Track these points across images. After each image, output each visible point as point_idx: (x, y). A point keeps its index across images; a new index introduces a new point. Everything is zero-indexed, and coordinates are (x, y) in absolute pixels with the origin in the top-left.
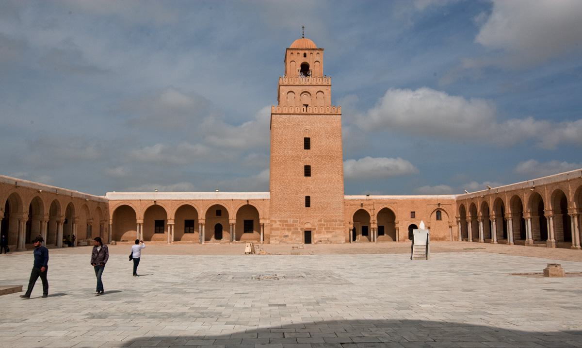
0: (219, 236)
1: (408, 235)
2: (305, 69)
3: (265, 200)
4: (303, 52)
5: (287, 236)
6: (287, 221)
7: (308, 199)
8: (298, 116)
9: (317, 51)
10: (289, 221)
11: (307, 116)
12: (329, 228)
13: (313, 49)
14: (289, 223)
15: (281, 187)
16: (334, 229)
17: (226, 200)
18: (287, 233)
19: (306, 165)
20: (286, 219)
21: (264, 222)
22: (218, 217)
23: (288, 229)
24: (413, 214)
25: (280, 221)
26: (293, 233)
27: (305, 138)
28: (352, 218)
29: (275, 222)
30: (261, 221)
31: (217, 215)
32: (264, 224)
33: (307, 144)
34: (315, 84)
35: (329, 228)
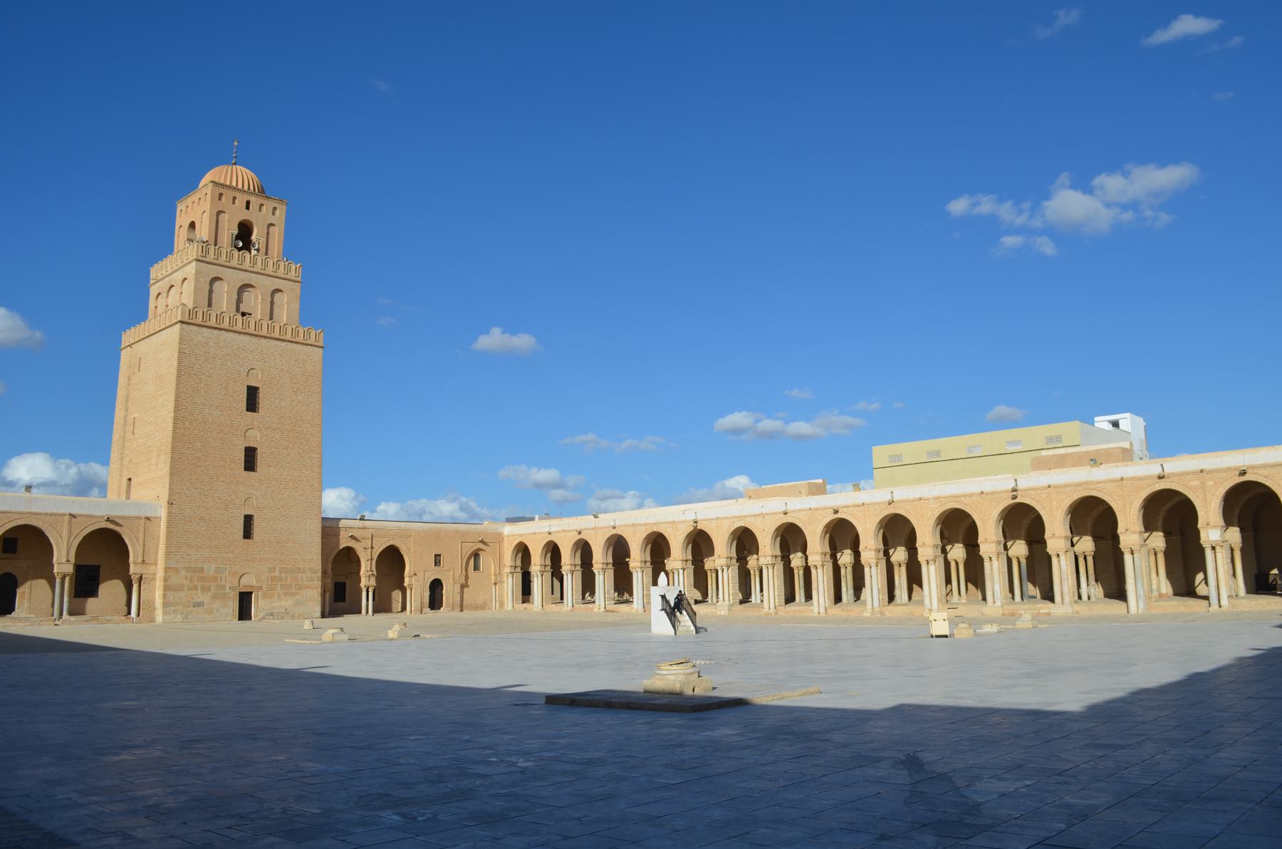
1: (427, 600)
4: (247, 198)
5: (200, 604)
6: (202, 570)
7: (248, 520)
8: (236, 336)
9: (274, 204)
11: (255, 340)
16: (300, 588)
17: (52, 515)
18: (200, 597)
22: (7, 555)
24: (437, 560)
25: (188, 569)
26: (214, 597)
29: (177, 570)
31: (5, 551)
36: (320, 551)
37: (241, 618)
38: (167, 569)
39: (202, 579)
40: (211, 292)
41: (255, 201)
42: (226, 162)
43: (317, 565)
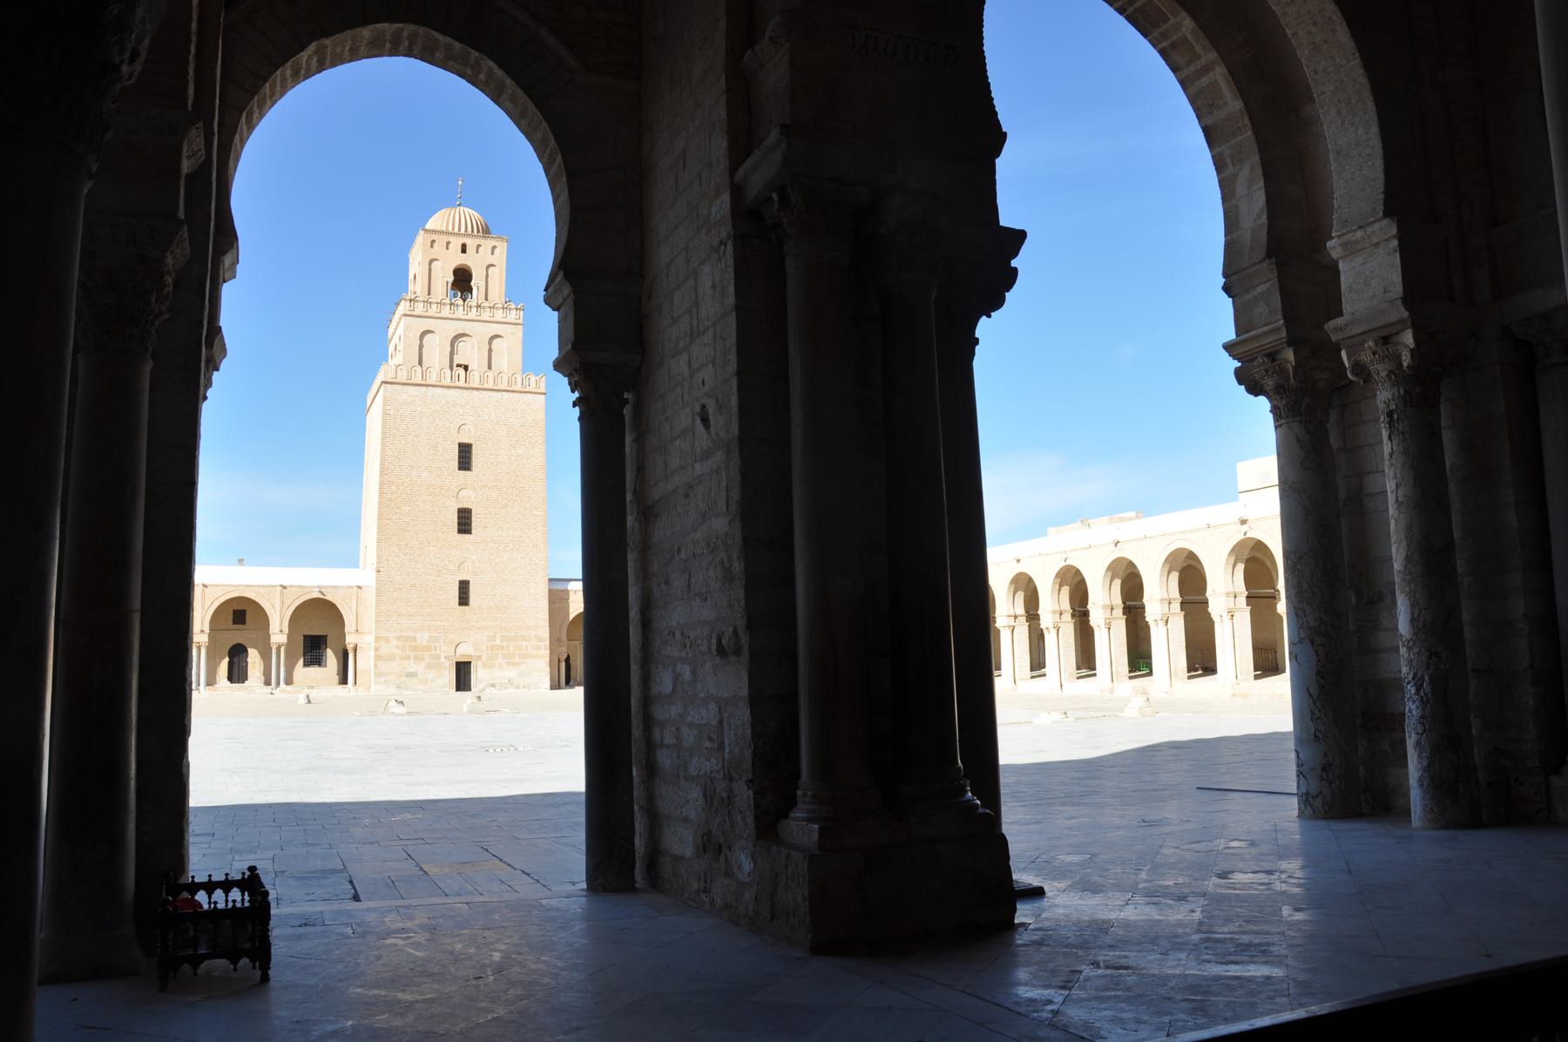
0: (237, 674)
2: (462, 281)
7: (464, 587)
9: (494, 243)
11: (465, 393)
18: (412, 666)
23: (416, 658)
25: (399, 638)
26: (429, 667)
29: (387, 640)
30: (350, 640)
31: (235, 622)
33: (465, 457)
36: (547, 617)
37: (458, 689)
38: (377, 638)
39: (415, 648)
40: (421, 347)
41: (471, 243)
42: (452, 205)
43: (544, 631)
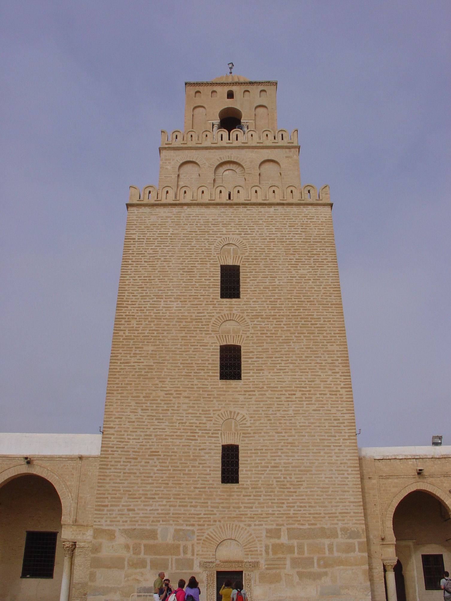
3: (88, 458)
6: (153, 534)
8: (203, 210)
9: (262, 88)
10: (159, 536)
11: (229, 211)
12: (309, 562)
13: (251, 83)
14: (160, 540)
15: (140, 411)
19: (225, 343)
20: (148, 527)
21: (79, 537)
25: (128, 533)
27: (222, 267)
28: (390, 524)
29: (111, 535)
30: (66, 534)
32: (74, 544)
33: (230, 283)
34: (254, 144)
35: (309, 562)
38: (98, 532)
